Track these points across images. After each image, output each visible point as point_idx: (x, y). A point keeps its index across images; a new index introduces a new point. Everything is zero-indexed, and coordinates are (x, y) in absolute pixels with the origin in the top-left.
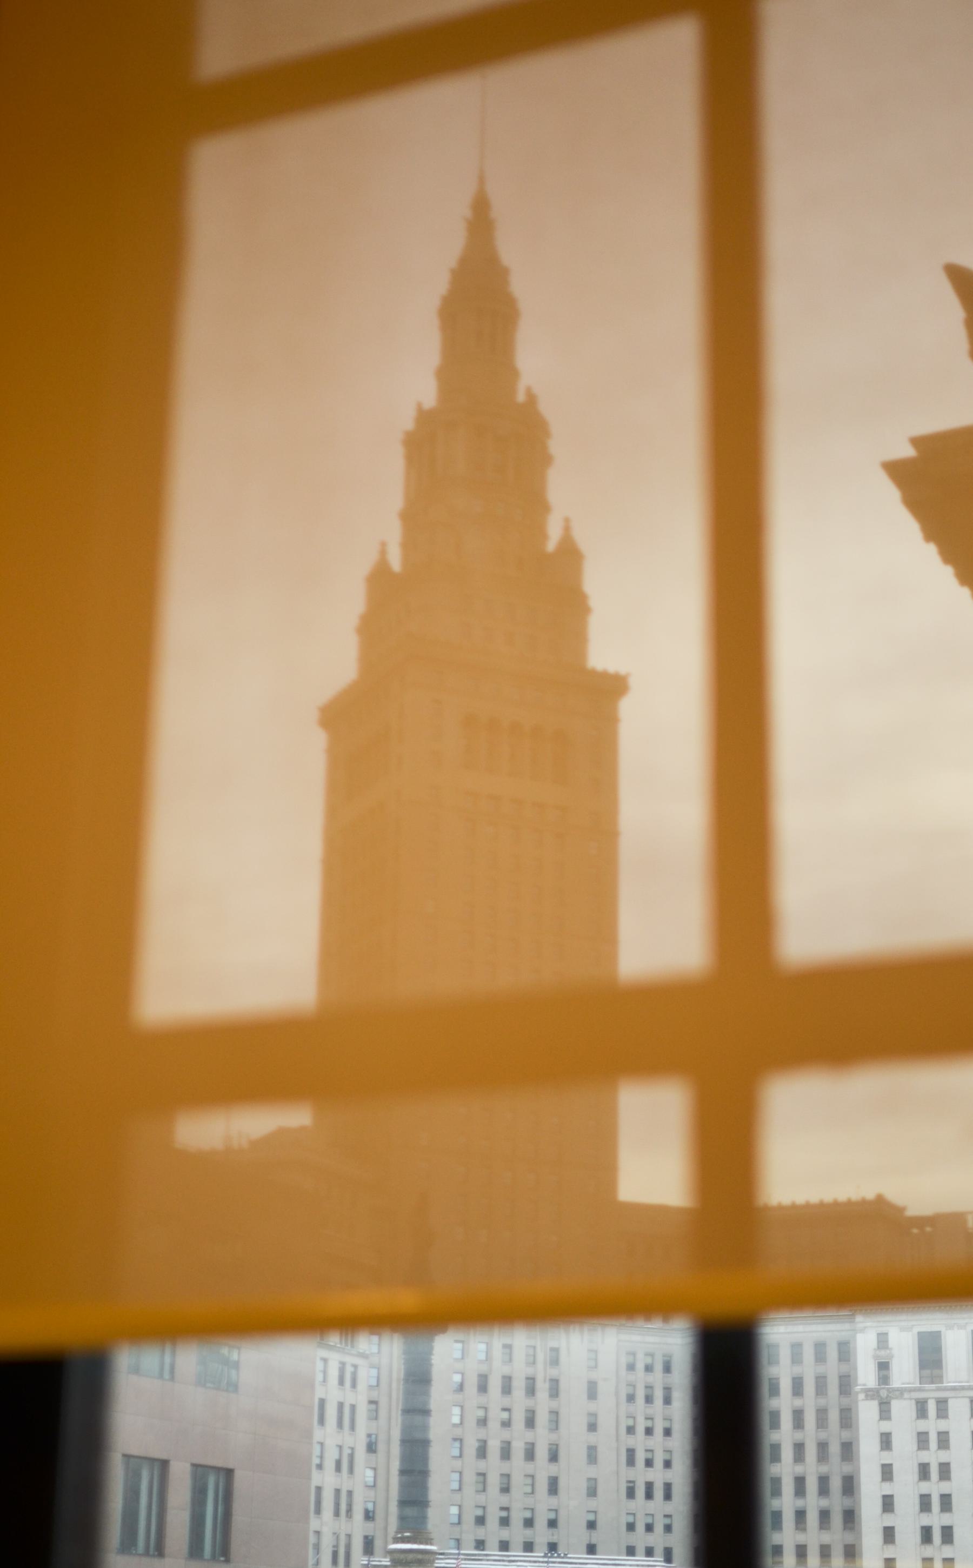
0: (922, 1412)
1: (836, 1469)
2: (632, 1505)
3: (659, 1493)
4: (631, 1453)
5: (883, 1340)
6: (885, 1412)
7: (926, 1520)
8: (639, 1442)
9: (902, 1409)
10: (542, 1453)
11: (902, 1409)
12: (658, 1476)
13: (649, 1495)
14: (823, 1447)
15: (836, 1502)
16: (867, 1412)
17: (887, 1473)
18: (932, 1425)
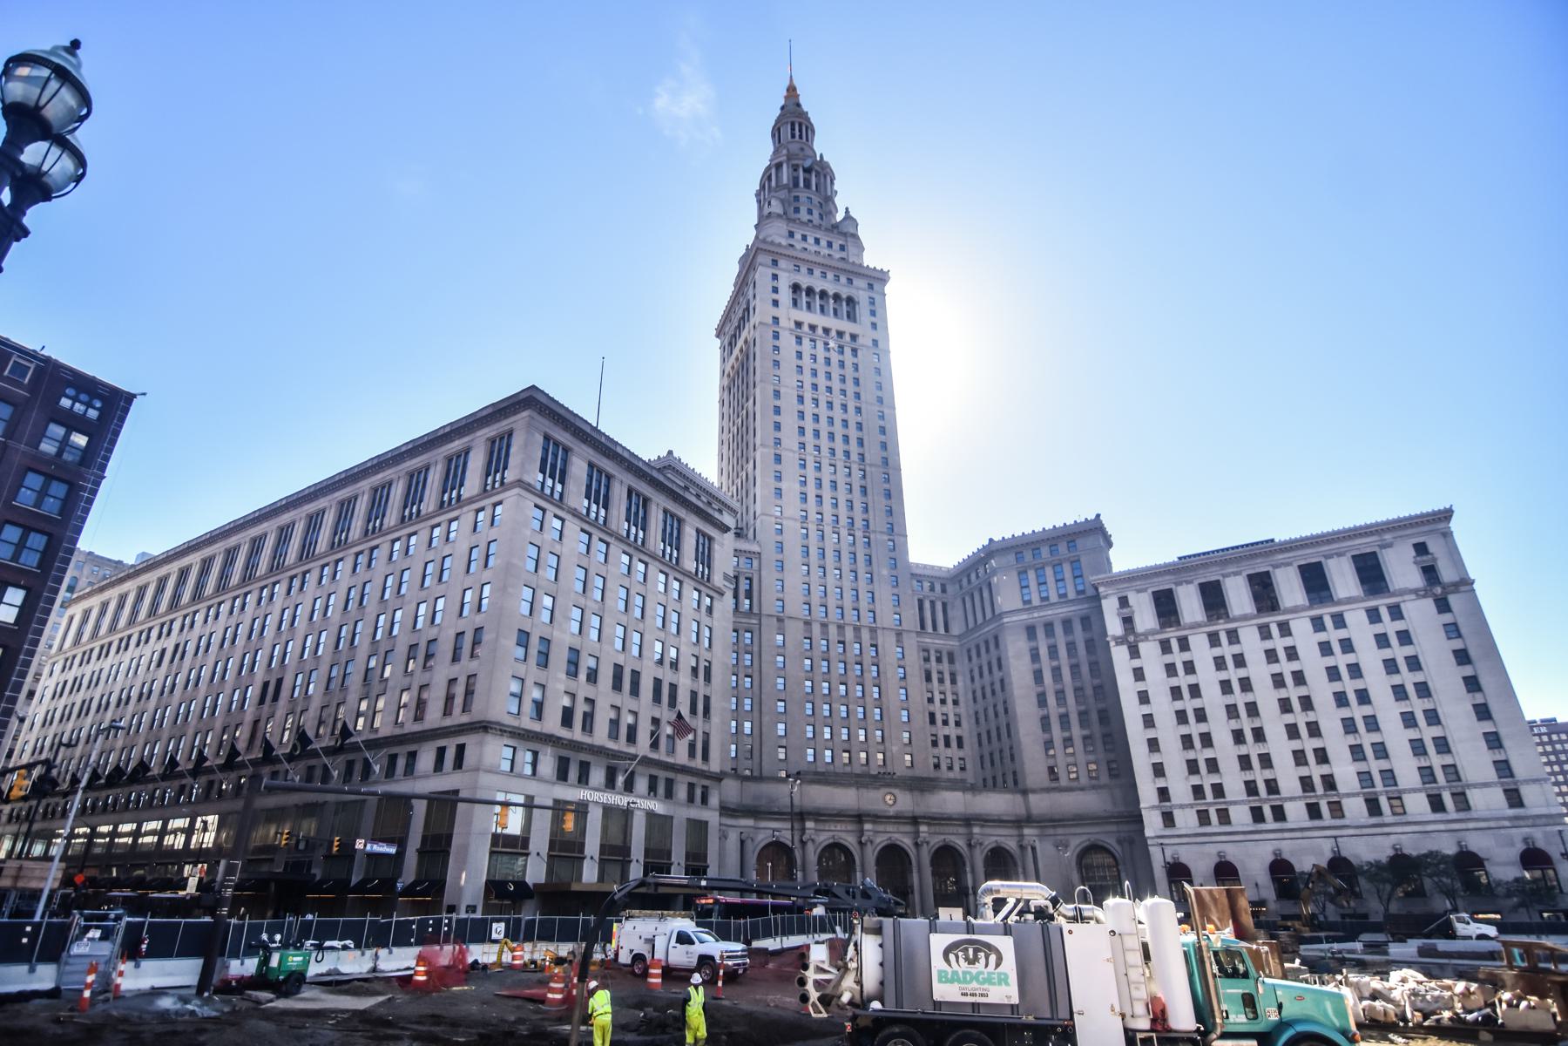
0: (1166, 647)
1: (1093, 706)
2: (936, 751)
3: (954, 743)
4: (932, 716)
5: (1124, 602)
6: (1134, 653)
7: (1184, 730)
8: (937, 707)
9: (1149, 649)
11: (1149, 649)
12: (951, 730)
13: (947, 744)
14: (1078, 690)
15: (1097, 729)
16: (1120, 655)
17: (1144, 698)
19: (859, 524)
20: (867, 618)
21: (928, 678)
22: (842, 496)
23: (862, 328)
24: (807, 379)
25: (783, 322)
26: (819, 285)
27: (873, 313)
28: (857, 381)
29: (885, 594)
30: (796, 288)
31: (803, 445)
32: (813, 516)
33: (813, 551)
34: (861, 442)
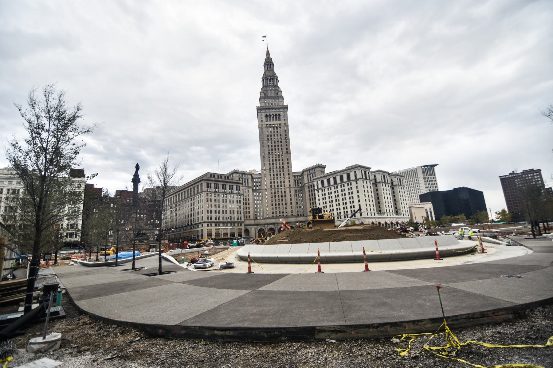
10: (284, 204)
11: (320, 191)
17: (319, 200)
18: (323, 193)
19: (281, 167)
20: (283, 186)
21: (296, 196)
22: (278, 162)
23: (282, 122)
24: (270, 138)
25: (264, 126)
26: (271, 114)
27: (284, 116)
28: (281, 135)
29: (287, 180)
30: (266, 116)
31: (269, 153)
32: (272, 168)
33: (272, 175)
34: (282, 149)
